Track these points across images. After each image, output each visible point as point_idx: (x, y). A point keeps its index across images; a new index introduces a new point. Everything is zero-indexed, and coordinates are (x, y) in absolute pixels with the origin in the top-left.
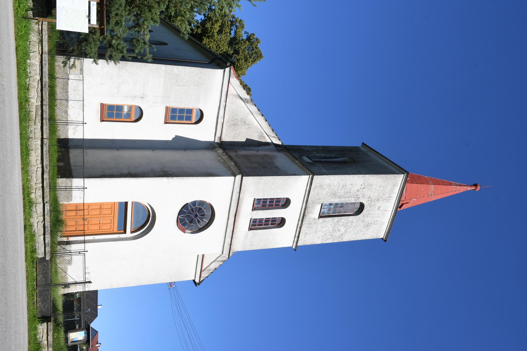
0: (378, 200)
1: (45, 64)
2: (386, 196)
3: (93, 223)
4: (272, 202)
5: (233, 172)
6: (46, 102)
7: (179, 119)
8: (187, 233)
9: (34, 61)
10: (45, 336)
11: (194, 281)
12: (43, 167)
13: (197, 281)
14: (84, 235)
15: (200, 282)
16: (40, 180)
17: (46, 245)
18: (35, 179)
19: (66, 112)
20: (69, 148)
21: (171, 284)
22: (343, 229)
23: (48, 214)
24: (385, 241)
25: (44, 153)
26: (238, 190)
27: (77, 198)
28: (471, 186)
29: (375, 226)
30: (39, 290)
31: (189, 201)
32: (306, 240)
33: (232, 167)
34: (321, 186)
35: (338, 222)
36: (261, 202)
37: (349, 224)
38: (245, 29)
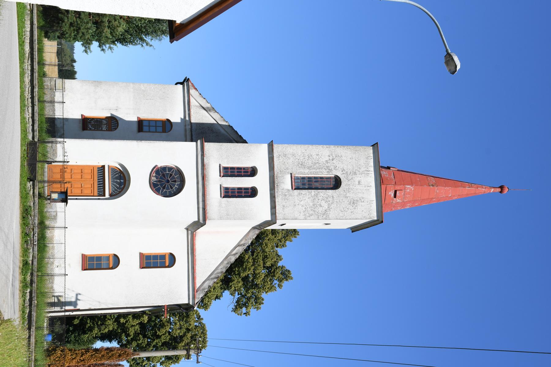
2: (363, 169)
3: (76, 186)
10: (32, 190)
29: (363, 204)
34: (285, 155)
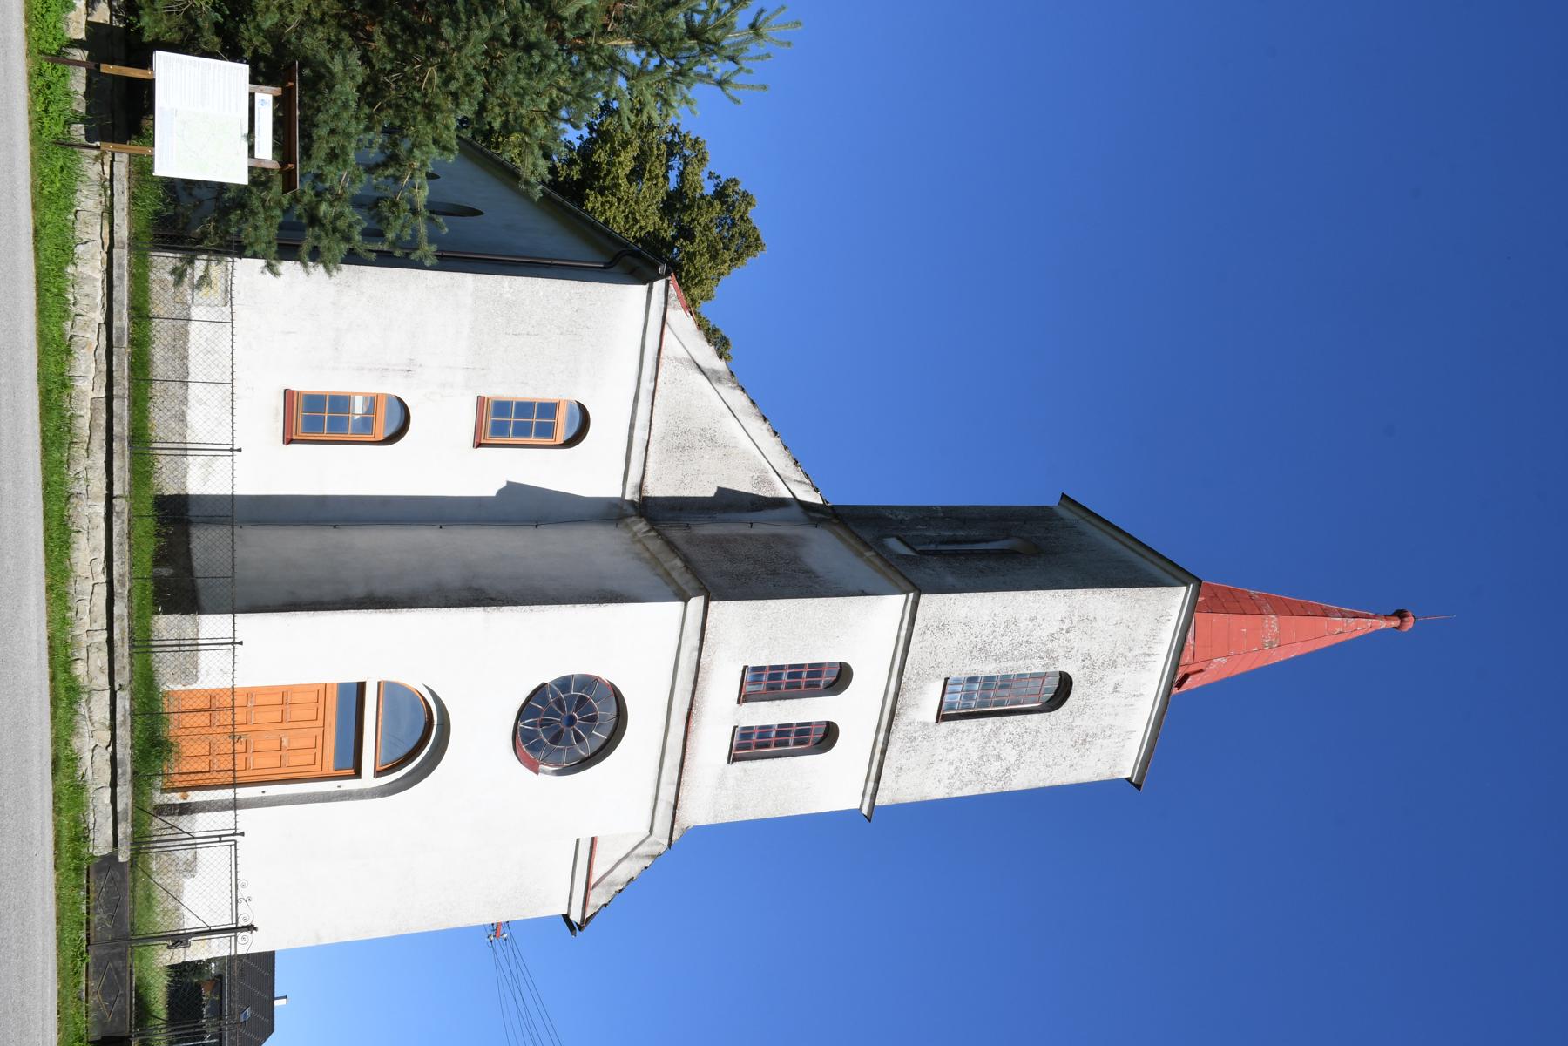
0: (1114, 664)
1: (121, 278)
2: (1137, 651)
3: (261, 746)
4: (798, 675)
5: (679, 588)
6: (122, 388)
7: (517, 433)
8: (545, 772)
9: (89, 267)
11: (566, 917)
12: (110, 583)
13: (576, 917)
14: (235, 785)
15: (586, 921)
16: (102, 622)
17: (120, 817)
18: (86, 619)
19: (182, 418)
20: (189, 523)
21: (496, 928)
22: (1010, 754)
23: (124, 722)
24: (1138, 786)
25: (115, 539)
26: (697, 643)
27: (212, 673)
28: (1386, 617)
30: (96, 957)
31: (548, 678)
32: (901, 788)
33: (675, 574)
34: (942, 627)
35: (995, 732)
36: (765, 678)
37: (1027, 738)
38: (710, 166)
